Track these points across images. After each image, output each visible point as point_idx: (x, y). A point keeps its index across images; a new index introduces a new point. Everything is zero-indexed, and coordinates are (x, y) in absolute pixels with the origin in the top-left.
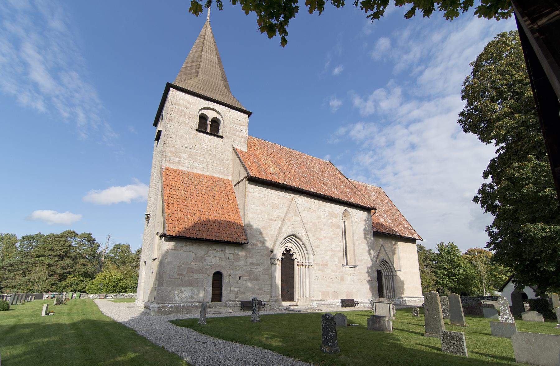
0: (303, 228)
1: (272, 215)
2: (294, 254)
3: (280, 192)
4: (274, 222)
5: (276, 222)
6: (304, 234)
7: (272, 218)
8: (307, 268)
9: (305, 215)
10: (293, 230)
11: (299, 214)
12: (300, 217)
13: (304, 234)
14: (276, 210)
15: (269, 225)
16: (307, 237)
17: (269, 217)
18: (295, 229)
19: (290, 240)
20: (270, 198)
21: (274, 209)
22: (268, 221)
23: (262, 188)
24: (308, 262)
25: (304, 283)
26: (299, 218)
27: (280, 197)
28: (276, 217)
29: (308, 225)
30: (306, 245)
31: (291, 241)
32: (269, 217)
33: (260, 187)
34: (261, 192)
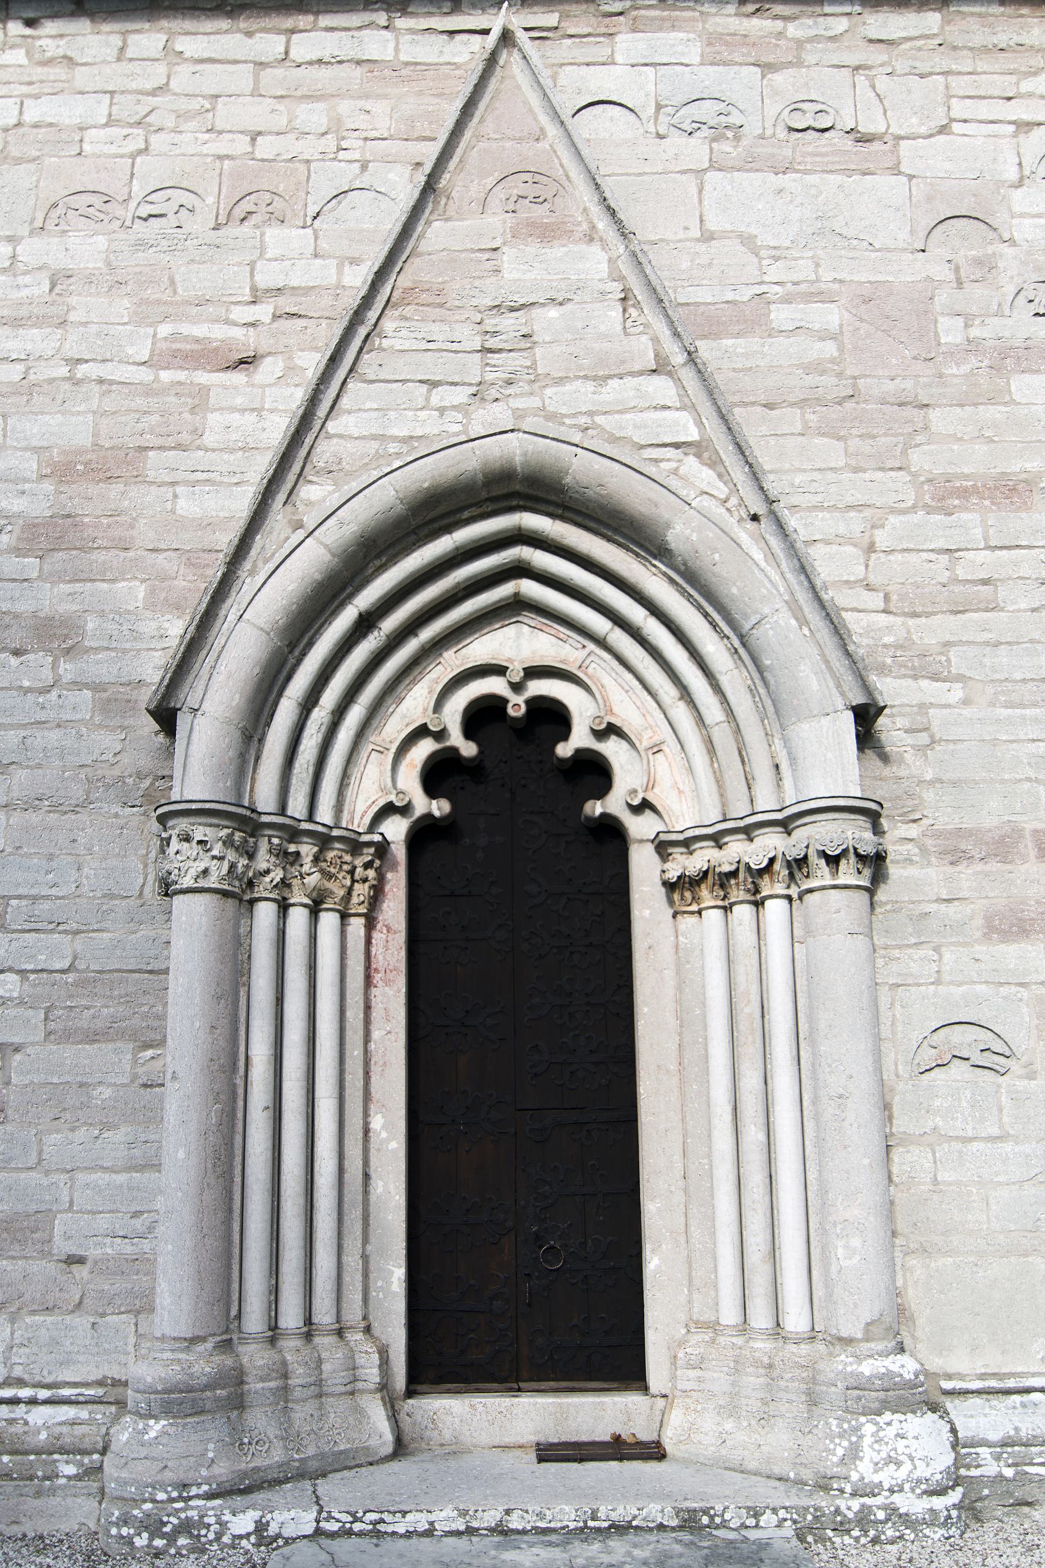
0: (660, 368)
1: (201, 303)
2: (612, 749)
3: (325, 20)
4: (238, 377)
5: (269, 369)
6: (696, 448)
7: (200, 331)
8: (775, 909)
9: (712, 225)
10: (498, 415)
11: (596, 211)
12: (611, 234)
13: (696, 448)
14: (273, 233)
15: (155, 419)
16: (739, 474)
17: (165, 330)
18: (520, 403)
19: (520, 570)
20: (181, 116)
21: (246, 228)
22: (144, 375)
23: (82, 25)
24: (786, 825)
25: (753, 1135)
26: (595, 248)
27: (324, 72)
28: (263, 312)
29: (772, 333)
30: (732, 590)
31: (530, 588)
32: (165, 330)
33: (50, 27)
34: (58, 72)
